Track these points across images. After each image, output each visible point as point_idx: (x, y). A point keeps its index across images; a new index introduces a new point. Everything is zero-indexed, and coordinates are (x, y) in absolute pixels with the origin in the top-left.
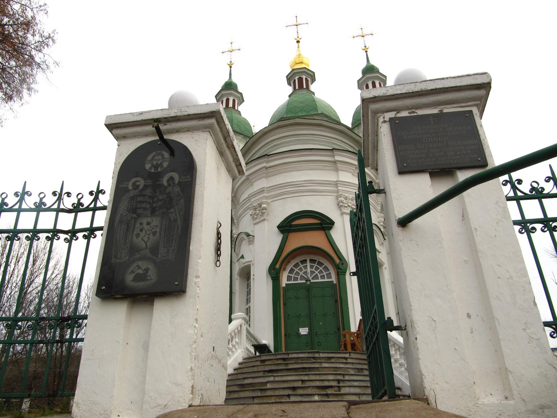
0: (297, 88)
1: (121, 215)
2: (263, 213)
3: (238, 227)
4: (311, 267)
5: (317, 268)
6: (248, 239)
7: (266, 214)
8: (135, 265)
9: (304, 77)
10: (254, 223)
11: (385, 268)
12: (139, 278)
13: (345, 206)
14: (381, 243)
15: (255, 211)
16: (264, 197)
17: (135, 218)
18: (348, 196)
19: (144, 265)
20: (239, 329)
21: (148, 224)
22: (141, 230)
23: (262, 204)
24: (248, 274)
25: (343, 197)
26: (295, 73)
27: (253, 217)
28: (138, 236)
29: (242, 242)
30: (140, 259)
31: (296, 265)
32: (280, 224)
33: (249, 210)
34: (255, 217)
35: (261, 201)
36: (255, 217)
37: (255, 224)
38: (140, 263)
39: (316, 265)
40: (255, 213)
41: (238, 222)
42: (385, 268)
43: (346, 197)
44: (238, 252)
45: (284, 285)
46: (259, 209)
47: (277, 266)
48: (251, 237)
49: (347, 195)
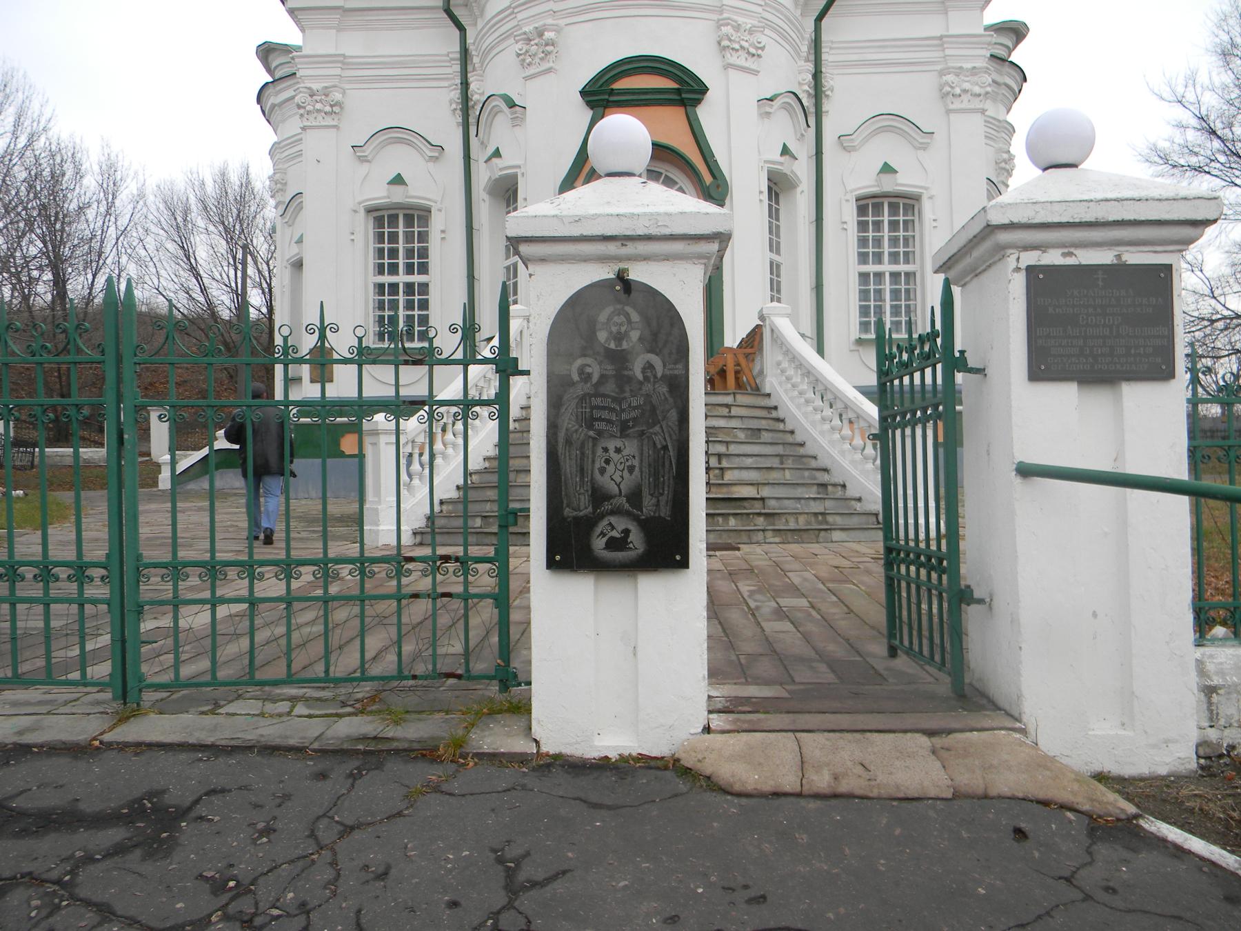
1: (567, 430)
2: (547, 54)
3: (482, 76)
6: (512, 114)
7: (552, 57)
8: (605, 522)
10: (524, 75)
11: (803, 191)
12: (613, 544)
13: (733, 49)
14: (799, 135)
15: (528, 44)
16: (548, 11)
17: (594, 439)
18: (743, 23)
19: (621, 523)
20: (519, 339)
21: (618, 450)
22: (607, 462)
23: (544, 30)
24: (507, 191)
25: (733, 26)
27: (524, 60)
28: (602, 471)
29: (495, 116)
30: (612, 513)
32: (585, 86)
33: (512, 40)
34: (527, 61)
35: (541, 23)
36: (529, 60)
37: (526, 78)
38: (613, 519)
40: (527, 51)
41: (482, 62)
42: (803, 191)
43: (739, 25)
44: (486, 138)
46: (536, 41)
48: (517, 108)
49: (741, 20)
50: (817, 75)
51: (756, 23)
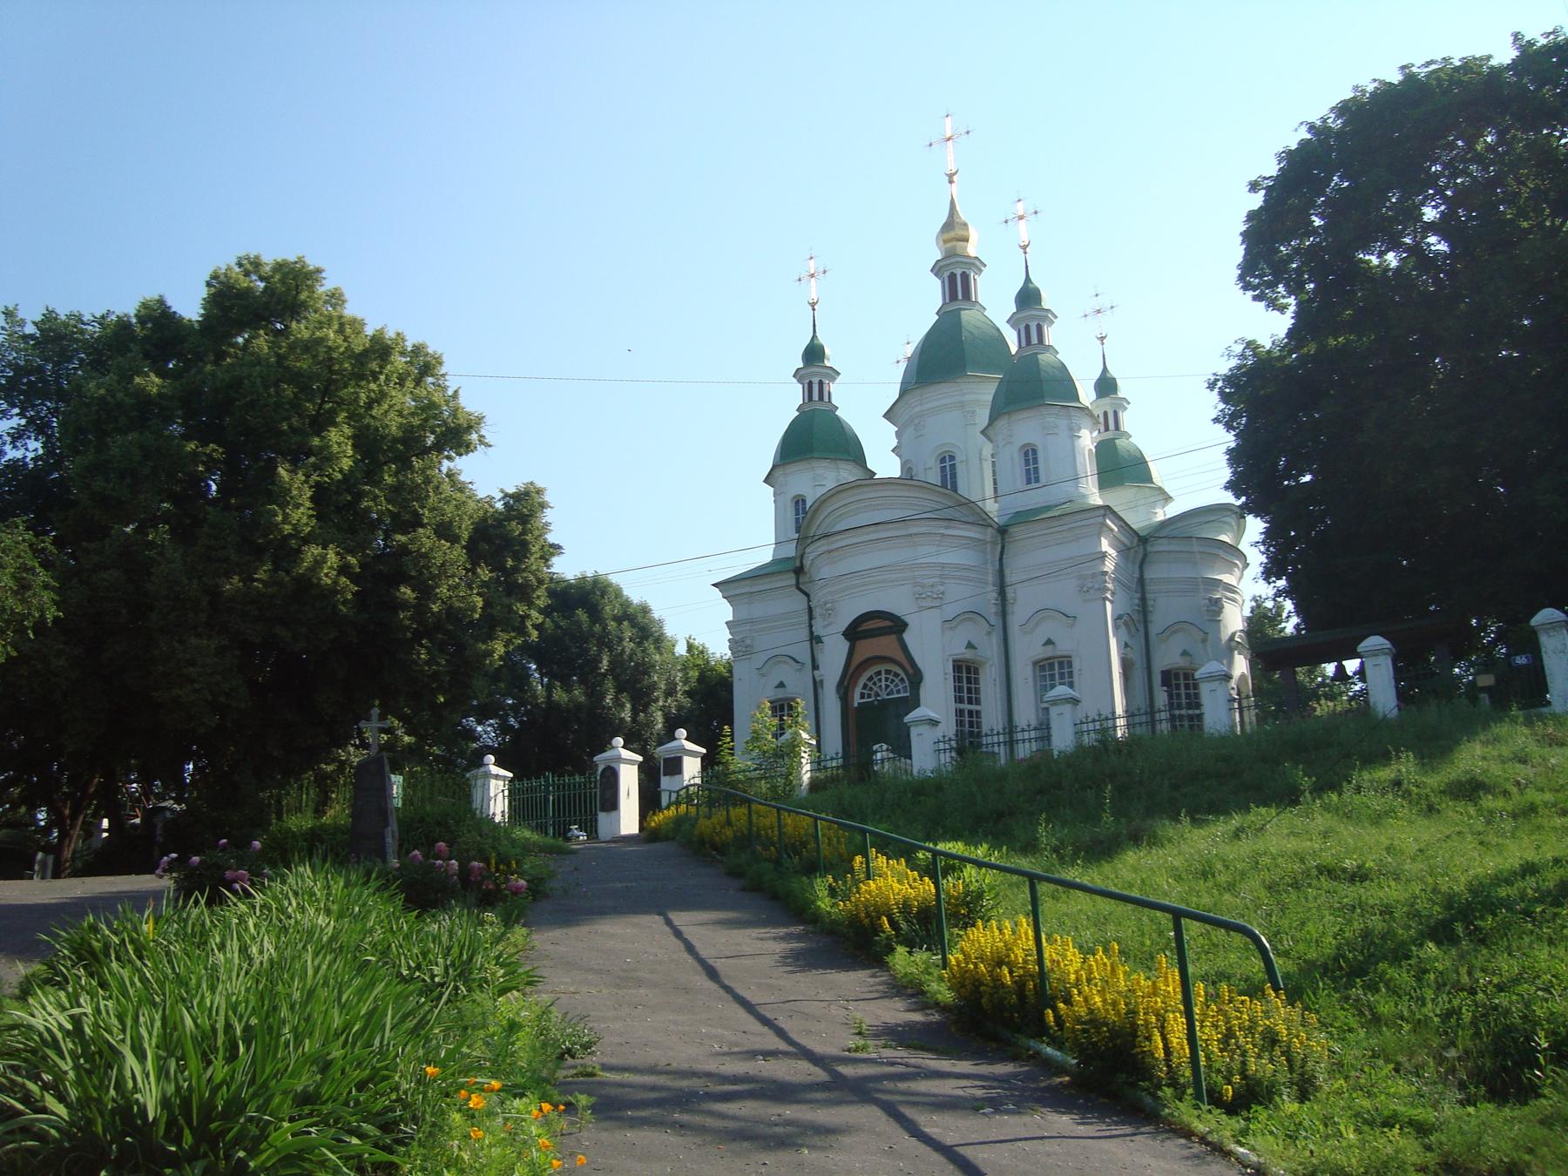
0: (947, 301)
4: (887, 679)
5: (893, 681)
9: (958, 272)
26: (940, 268)
31: (870, 679)
39: (891, 677)
42: (991, 666)
45: (856, 705)
47: (846, 683)
49: (925, 581)
50: (1002, 593)
51: (937, 580)
